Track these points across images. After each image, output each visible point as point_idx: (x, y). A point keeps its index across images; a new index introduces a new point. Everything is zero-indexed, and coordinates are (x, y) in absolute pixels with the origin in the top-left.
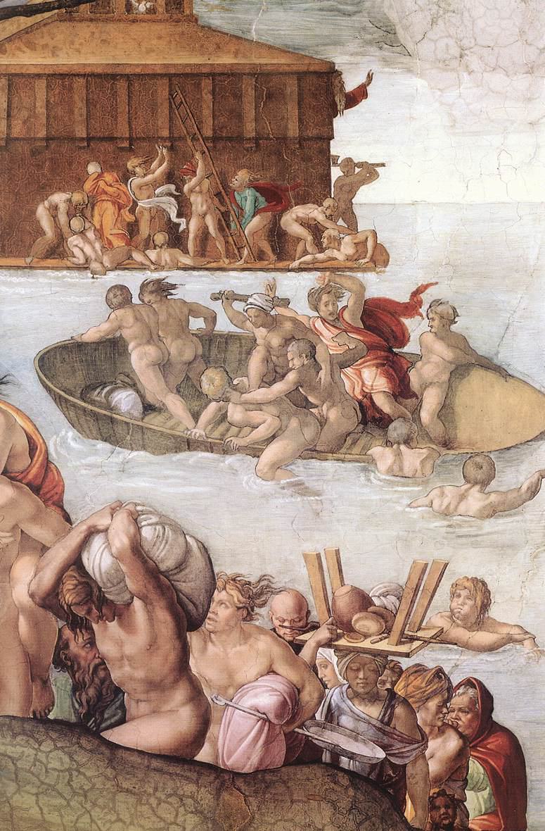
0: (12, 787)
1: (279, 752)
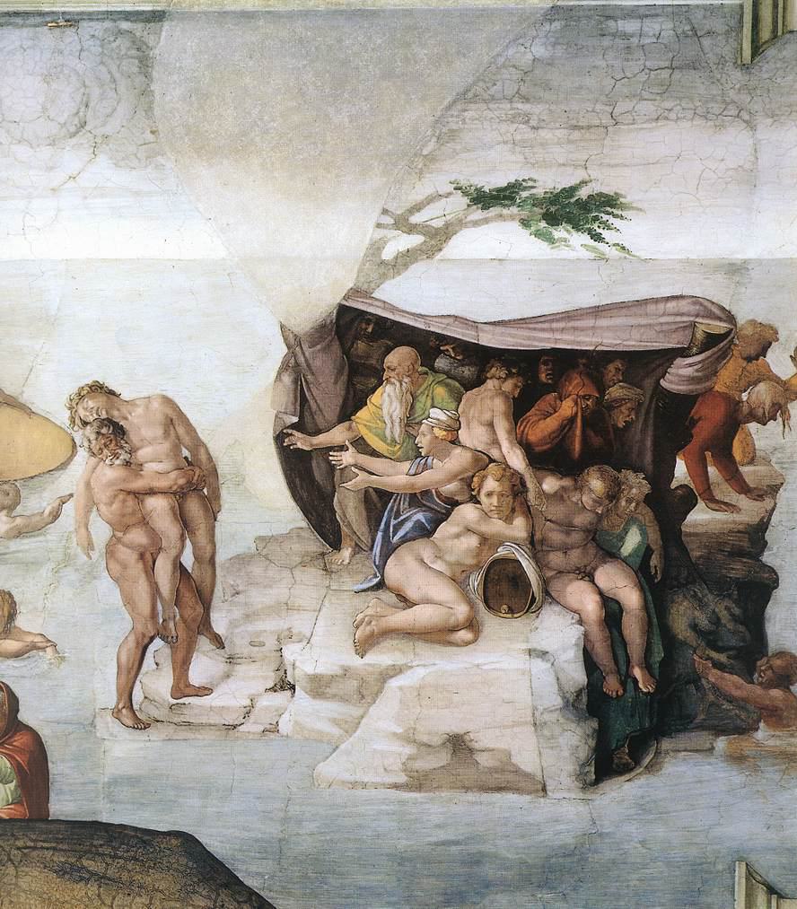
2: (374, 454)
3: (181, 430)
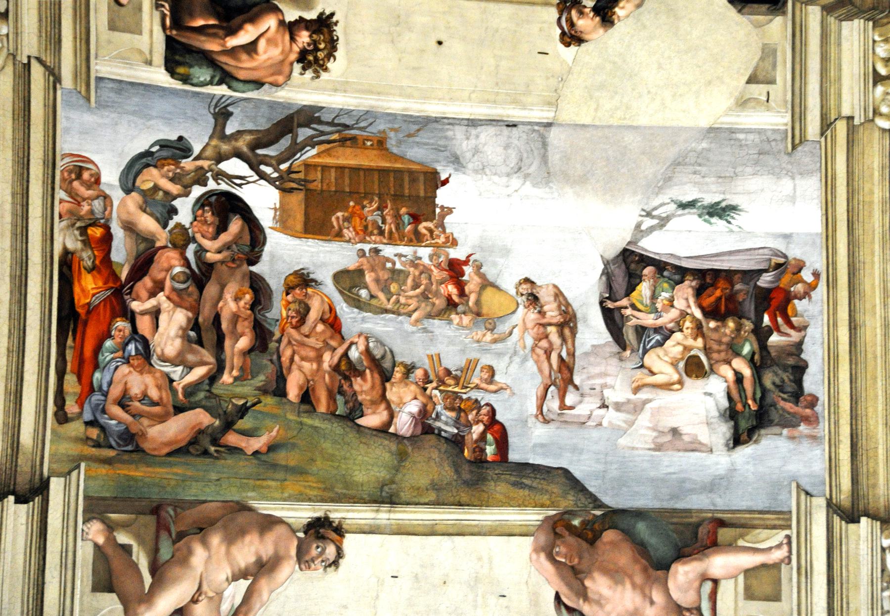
0: (322, 440)
1: (419, 430)
2: (639, 310)
3: (561, 299)
